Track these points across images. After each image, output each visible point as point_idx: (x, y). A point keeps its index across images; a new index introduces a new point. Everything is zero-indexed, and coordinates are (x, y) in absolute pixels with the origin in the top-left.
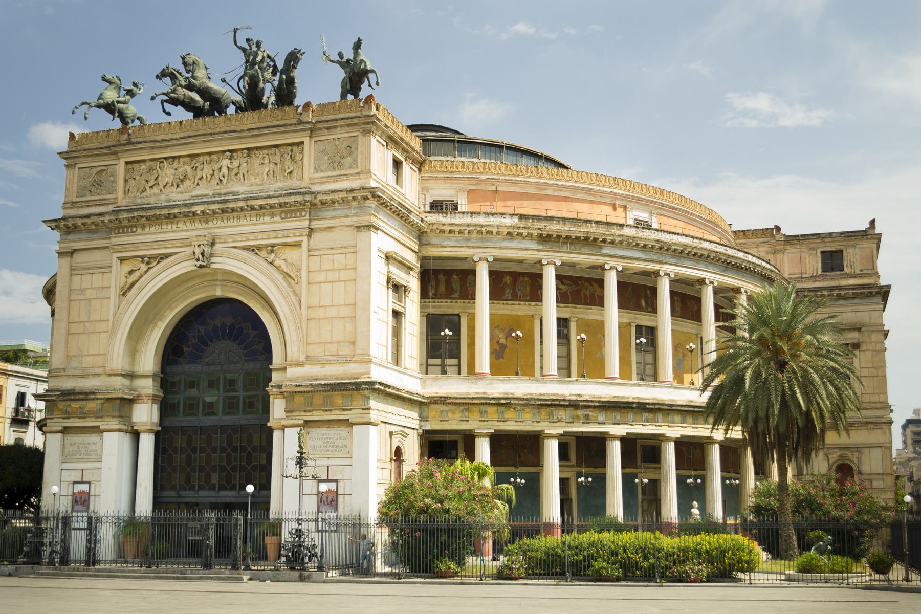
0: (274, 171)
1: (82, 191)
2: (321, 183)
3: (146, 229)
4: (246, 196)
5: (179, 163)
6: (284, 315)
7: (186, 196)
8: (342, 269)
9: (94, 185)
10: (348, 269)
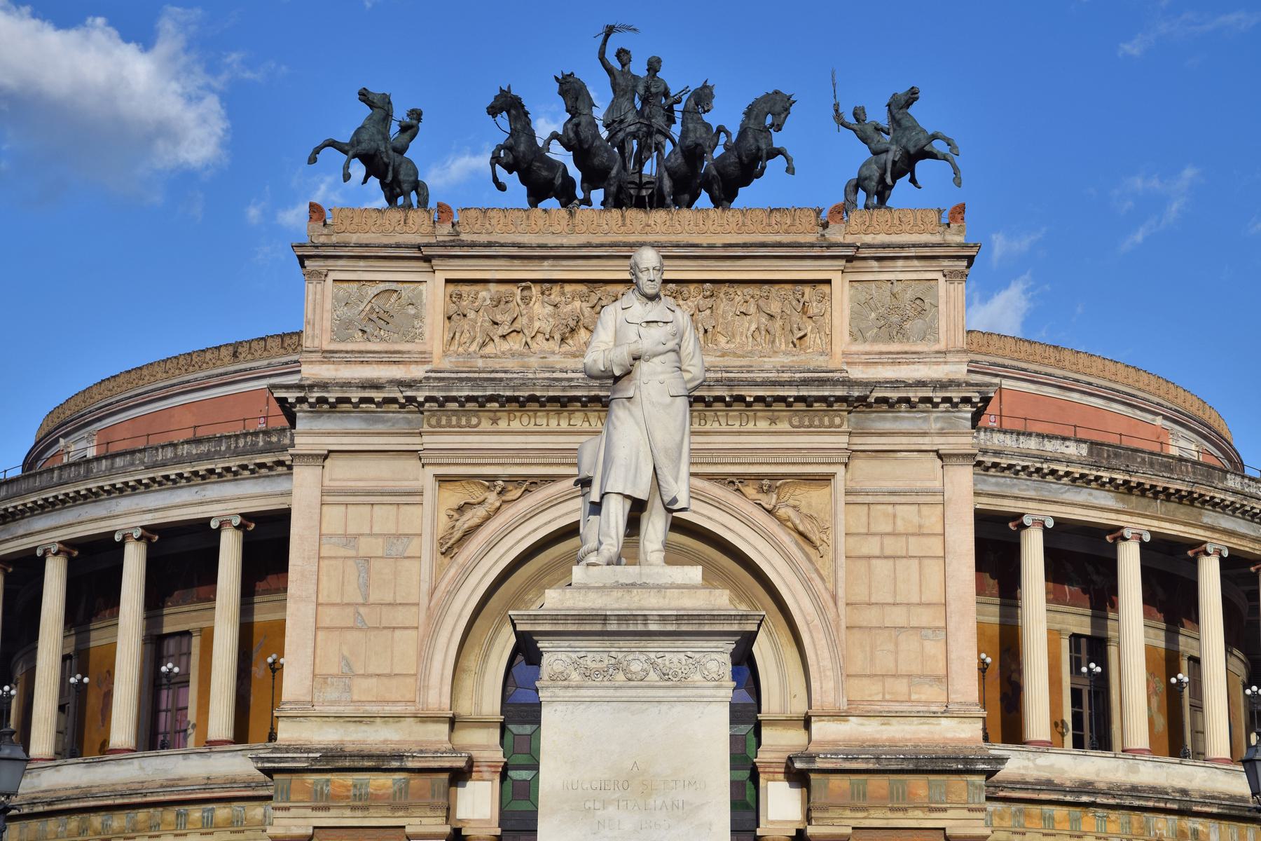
0: (767, 331)
1: (343, 329)
2: (867, 364)
3: (499, 422)
4: (719, 375)
5: (563, 294)
6: (805, 617)
8: (913, 535)
10: (923, 534)
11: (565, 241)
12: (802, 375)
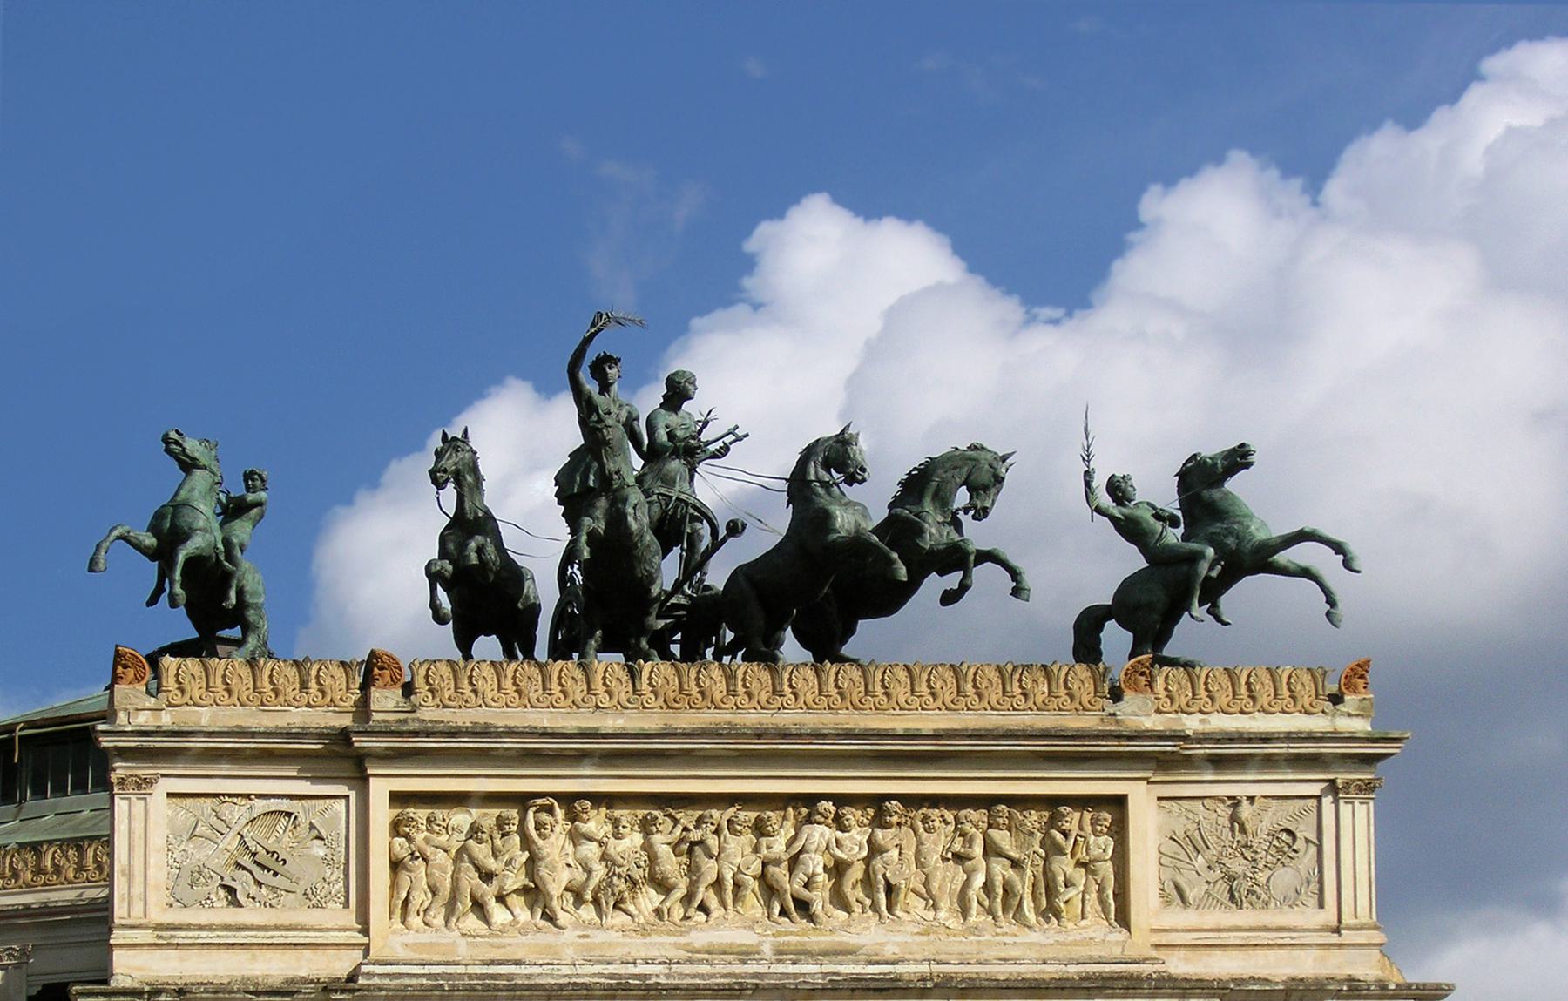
4: (924, 969)
7: (663, 945)
9: (239, 866)
11: (611, 723)
12: (1080, 968)
